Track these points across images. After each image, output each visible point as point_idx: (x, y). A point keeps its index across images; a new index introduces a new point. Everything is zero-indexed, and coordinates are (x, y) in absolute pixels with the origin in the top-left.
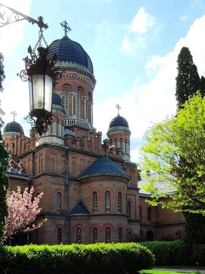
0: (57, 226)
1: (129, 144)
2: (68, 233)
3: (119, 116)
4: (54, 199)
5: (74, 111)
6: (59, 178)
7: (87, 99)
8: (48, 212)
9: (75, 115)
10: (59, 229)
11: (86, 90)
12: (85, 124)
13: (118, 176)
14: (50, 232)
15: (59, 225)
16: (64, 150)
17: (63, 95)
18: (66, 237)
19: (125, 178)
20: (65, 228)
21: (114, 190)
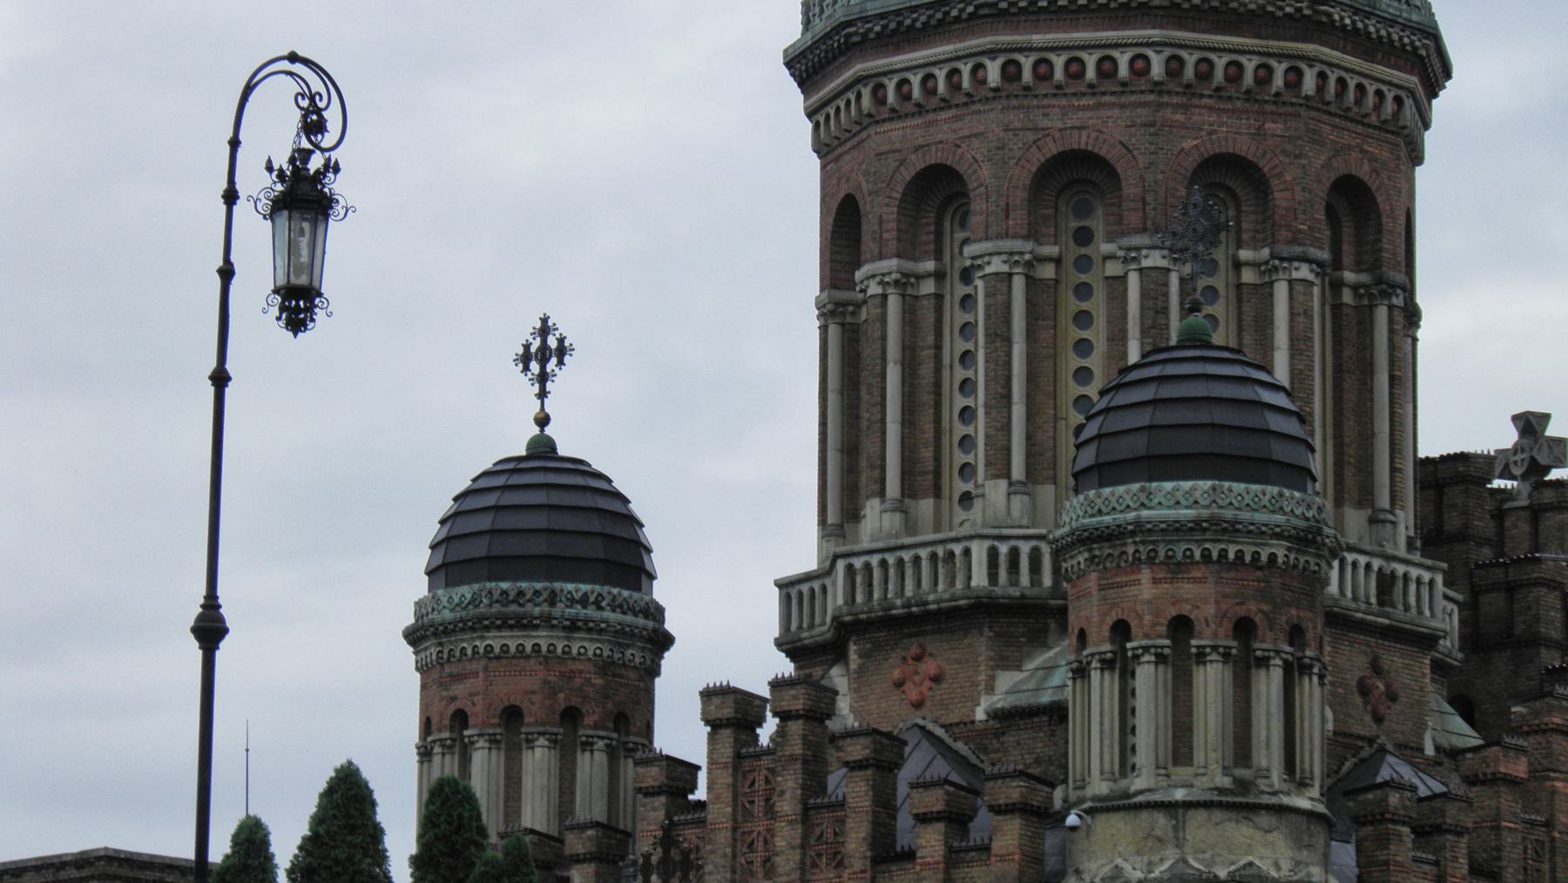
7: (997, 266)
9: (882, 493)
11: (986, 172)
12: (925, 564)
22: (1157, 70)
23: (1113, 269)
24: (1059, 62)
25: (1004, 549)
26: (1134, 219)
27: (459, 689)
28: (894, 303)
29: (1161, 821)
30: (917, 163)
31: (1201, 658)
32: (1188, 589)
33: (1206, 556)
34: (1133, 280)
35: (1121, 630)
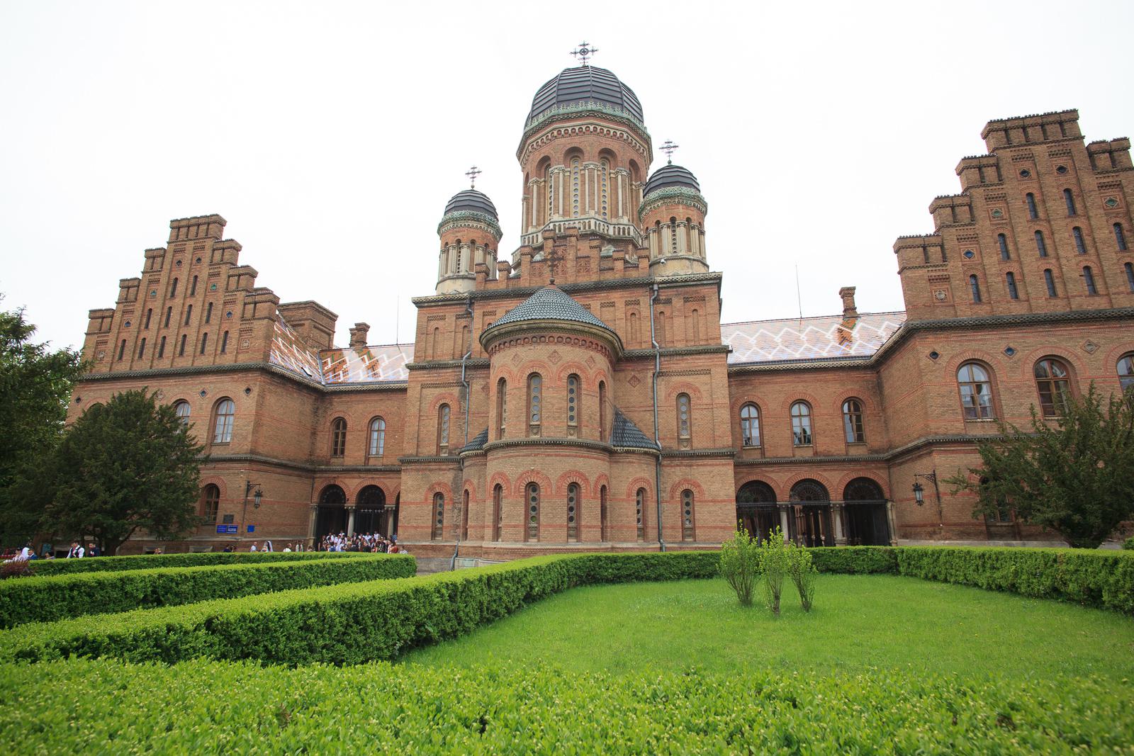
0: (431, 489)
1: (702, 233)
2: (460, 506)
3: (670, 166)
4: (431, 422)
5: (557, 207)
6: (444, 371)
7: (592, 166)
8: (412, 455)
10: (439, 495)
11: (588, 148)
13: (521, 330)
14: (411, 503)
15: (439, 484)
16: (461, 302)
17: (543, 184)
18: (455, 516)
19: (545, 328)
20: (455, 493)
21: (515, 370)
22: (625, 137)
23: (612, 175)
24: (605, 130)
25: (598, 222)
26: (620, 164)
27: (459, 234)
28: (561, 175)
29: (687, 262)
30: (570, 146)
31: (693, 228)
32: (690, 212)
33: (694, 205)
34: (620, 177)
35: (673, 220)
